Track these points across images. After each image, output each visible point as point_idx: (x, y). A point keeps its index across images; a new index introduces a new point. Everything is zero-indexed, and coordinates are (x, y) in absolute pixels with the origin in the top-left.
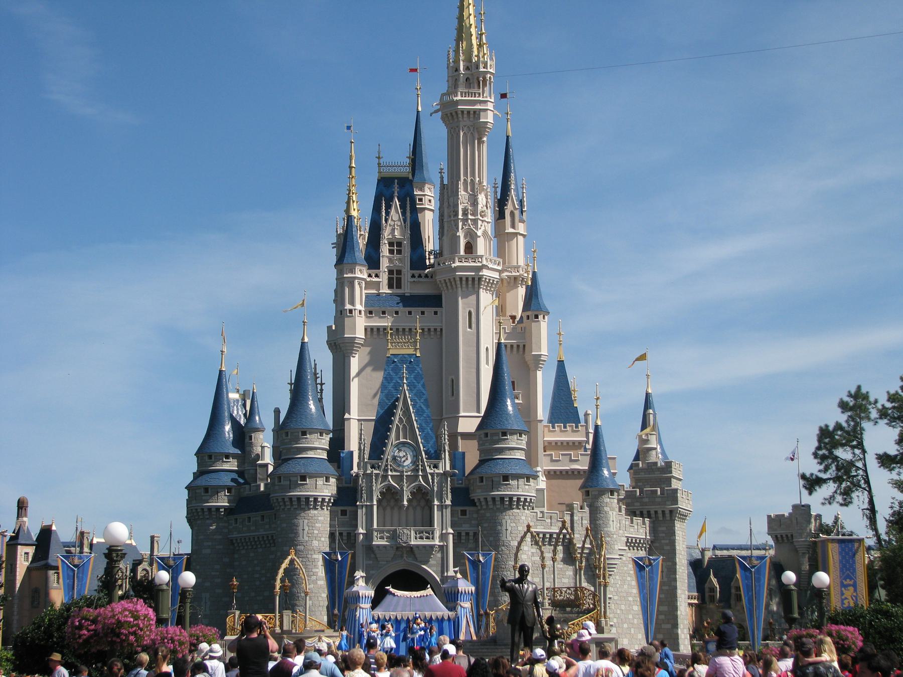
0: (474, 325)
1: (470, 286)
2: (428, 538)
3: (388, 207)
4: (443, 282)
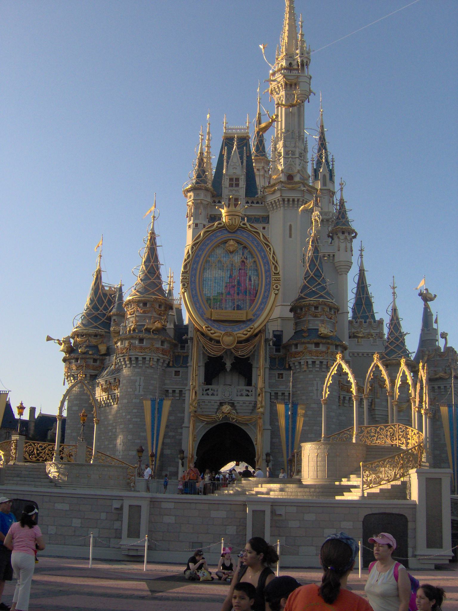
0: (293, 236)
1: (291, 205)
2: (248, 395)
3: (229, 153)
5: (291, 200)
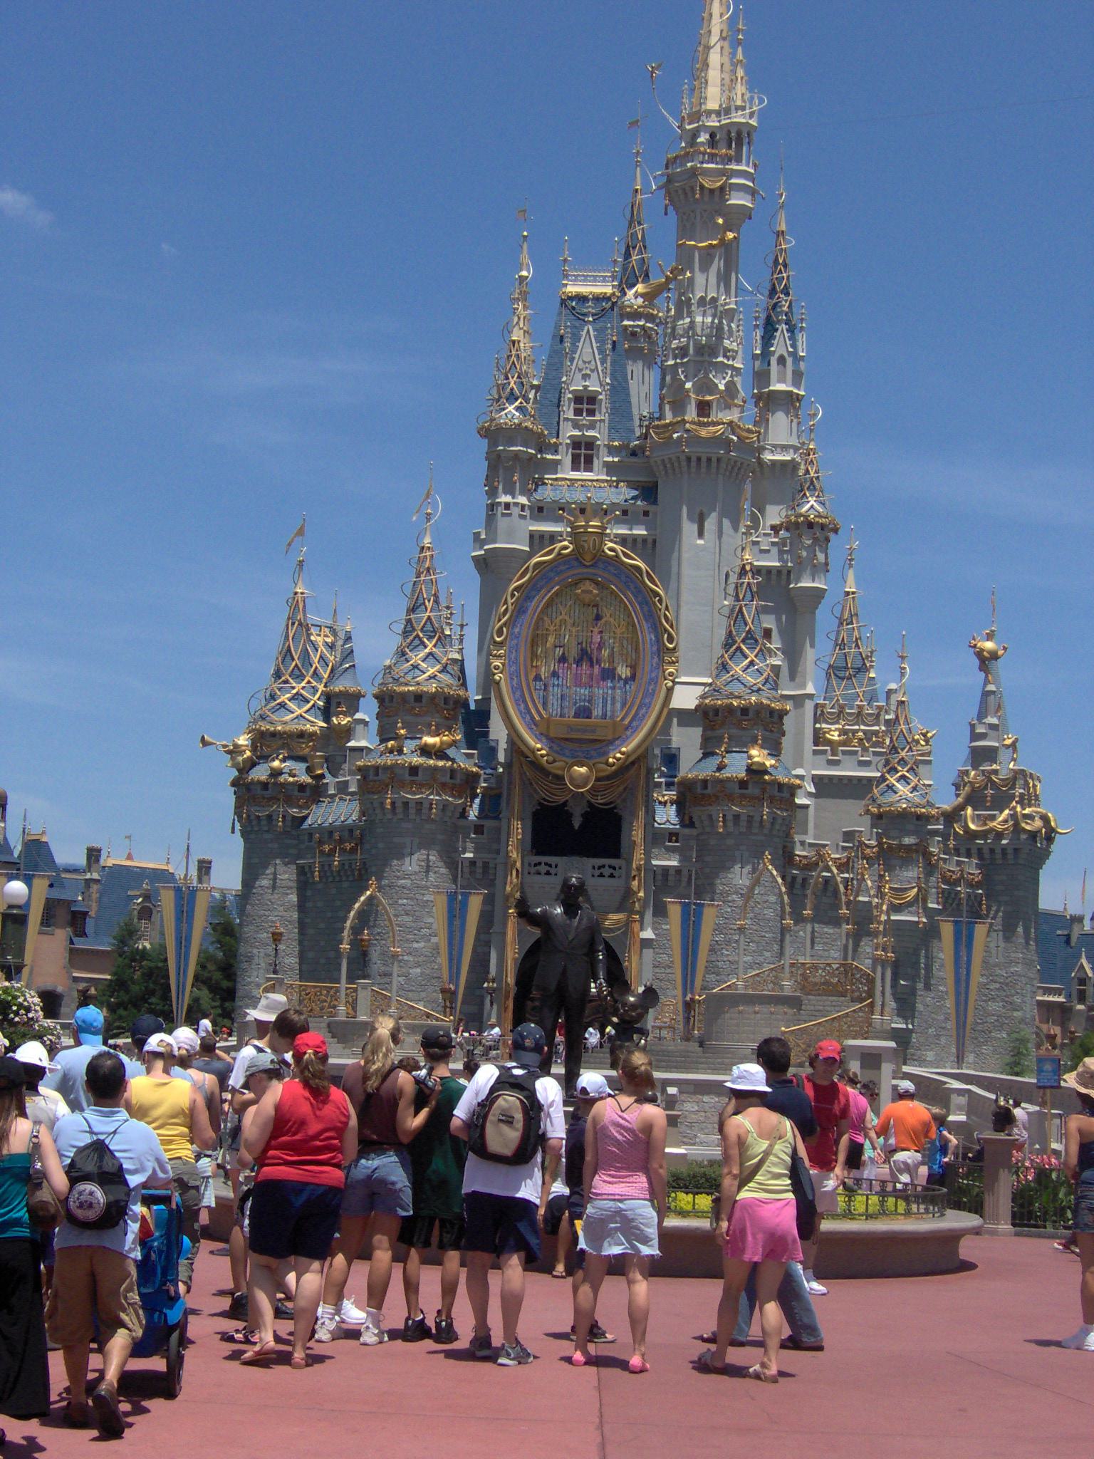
4: (659, 462)
5: (704, 459)
